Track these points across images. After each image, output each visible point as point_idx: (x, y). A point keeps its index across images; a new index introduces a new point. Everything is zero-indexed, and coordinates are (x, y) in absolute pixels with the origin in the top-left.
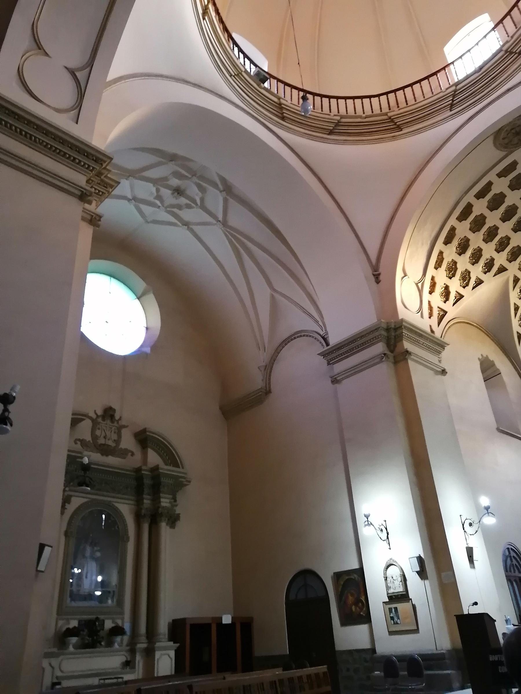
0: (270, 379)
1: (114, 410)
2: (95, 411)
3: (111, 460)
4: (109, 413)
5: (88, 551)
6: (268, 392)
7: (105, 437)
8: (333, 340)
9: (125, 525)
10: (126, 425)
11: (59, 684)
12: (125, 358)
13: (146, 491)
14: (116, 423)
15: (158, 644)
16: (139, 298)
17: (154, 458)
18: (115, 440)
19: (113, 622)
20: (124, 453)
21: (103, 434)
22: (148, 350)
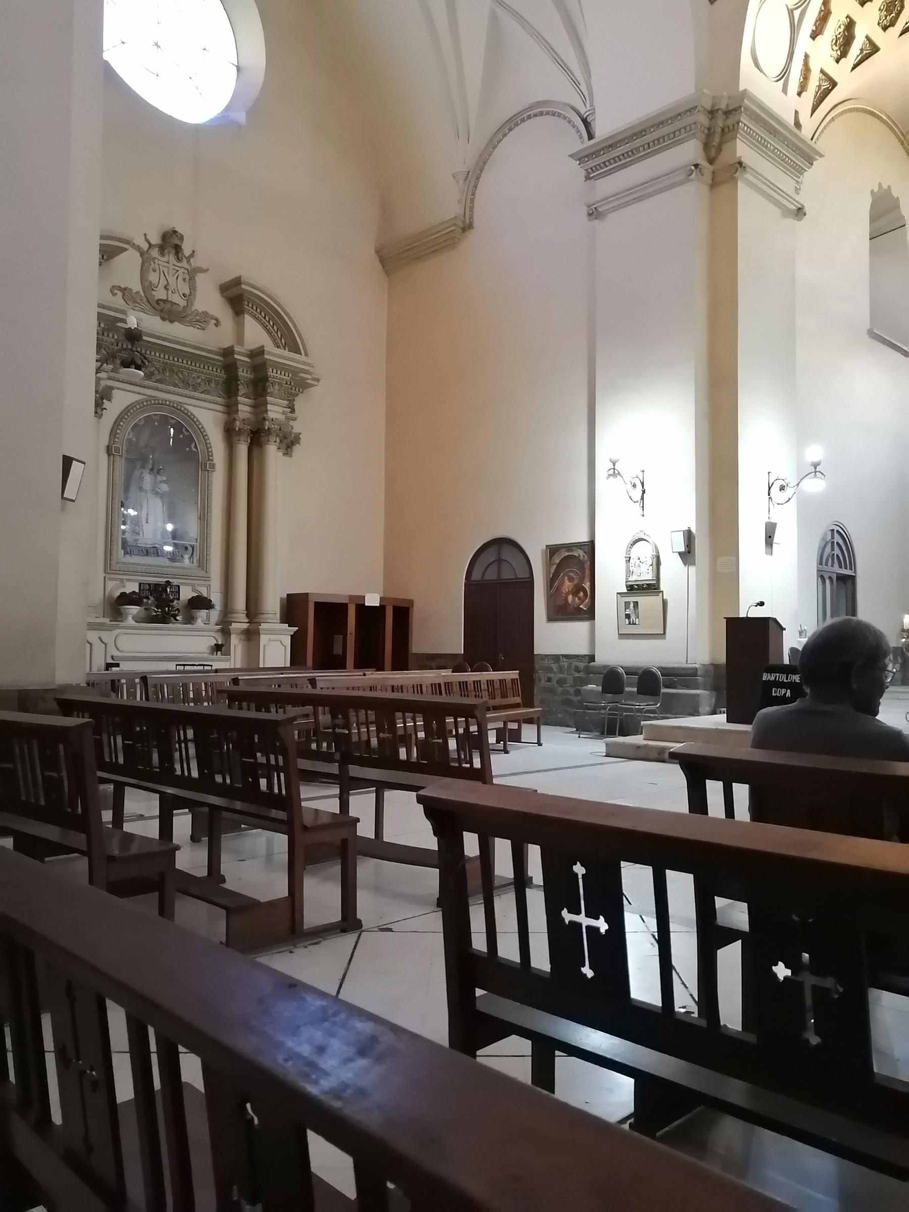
0: (472, 201)
1: (181, 238)
2: (145, 235)
3: (179, 332)
4: (171, 242)
5: (148, 479)
6: (468, 227)
7: (166, 288)
8: (602, 130)
9: (208, 446)
10: (205, 267)
11: (117, 665)
12: (197, 128)
13: (242, 390)
14: (185, 261)
15: (263, 626)
17: (255, 334)
18: (184, 295)
19: (194, 590)
20: (203, 320)
21: (163, 282)
22: (240, 117)
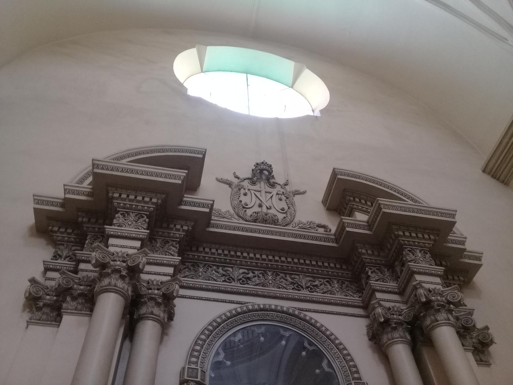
1: (269, 168)
4: (263, 173)
7: (260, 206)
9: (347, 358)
16: (292, 87)
18: (283, 209)
